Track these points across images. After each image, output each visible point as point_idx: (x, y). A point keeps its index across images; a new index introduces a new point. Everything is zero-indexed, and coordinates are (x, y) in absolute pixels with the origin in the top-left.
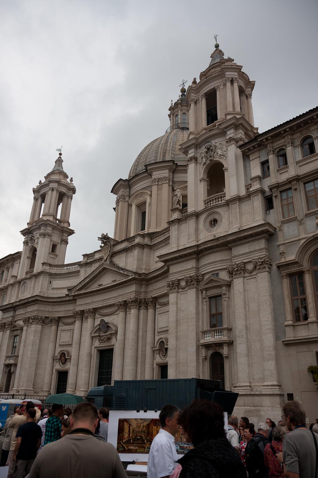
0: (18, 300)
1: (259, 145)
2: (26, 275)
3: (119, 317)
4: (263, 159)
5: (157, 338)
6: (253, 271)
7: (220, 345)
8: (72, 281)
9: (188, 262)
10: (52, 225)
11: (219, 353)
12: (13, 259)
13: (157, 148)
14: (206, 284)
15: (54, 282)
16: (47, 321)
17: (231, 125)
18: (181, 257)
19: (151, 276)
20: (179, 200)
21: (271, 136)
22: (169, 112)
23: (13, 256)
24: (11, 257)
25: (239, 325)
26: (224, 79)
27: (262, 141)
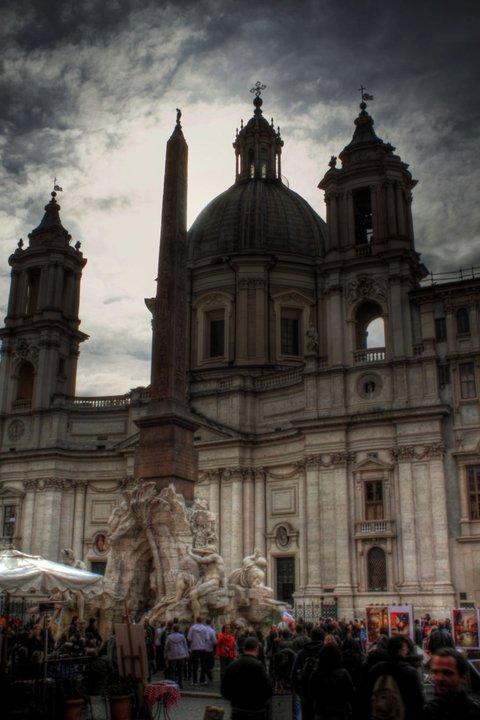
0: (8, 449)
3: (208, 490)
4: (439, 315)
5: (271, 523)
6: (424, 456)
7: (383, 539)
8: (106, 425)
9: (335, 434)
11: (381, 549)
14: (363, 465)
16: (68, 485)
17: (397, 257)
18: (325, 426)
19: (263, 438)
22: (234, 139)
25: (406, 517)
26: (383, 177)
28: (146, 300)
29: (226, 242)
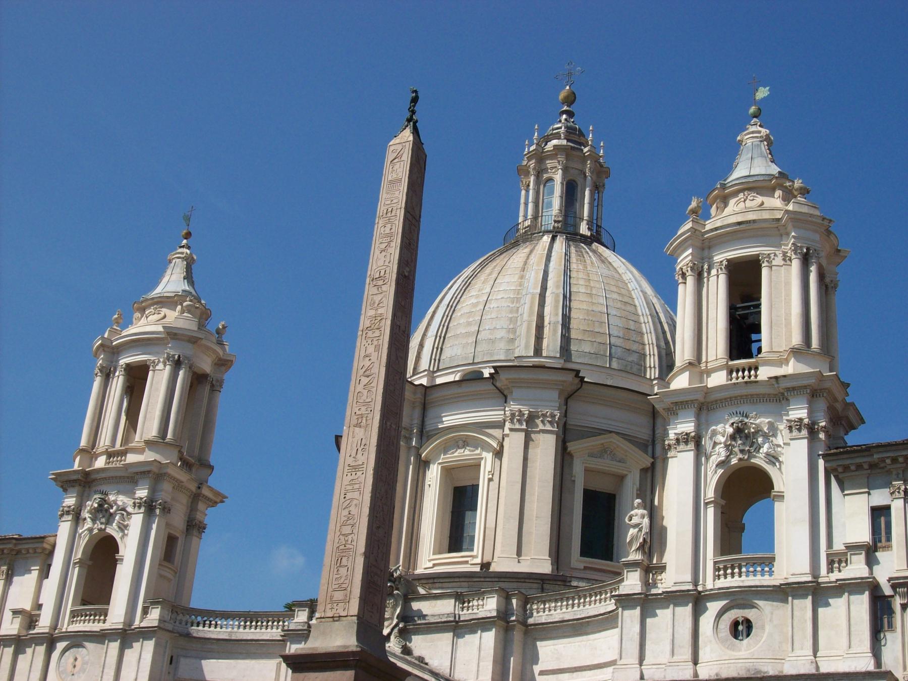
1: (872, 466)
2: (74, 617)
10: (174, 479)
12: (14, 553)
15: (183, 661)
17: (805, 387)
20: (644, 538)
23: (15, 545)
24: (10, 546)
27: (883, 460)
29: (492, 341)
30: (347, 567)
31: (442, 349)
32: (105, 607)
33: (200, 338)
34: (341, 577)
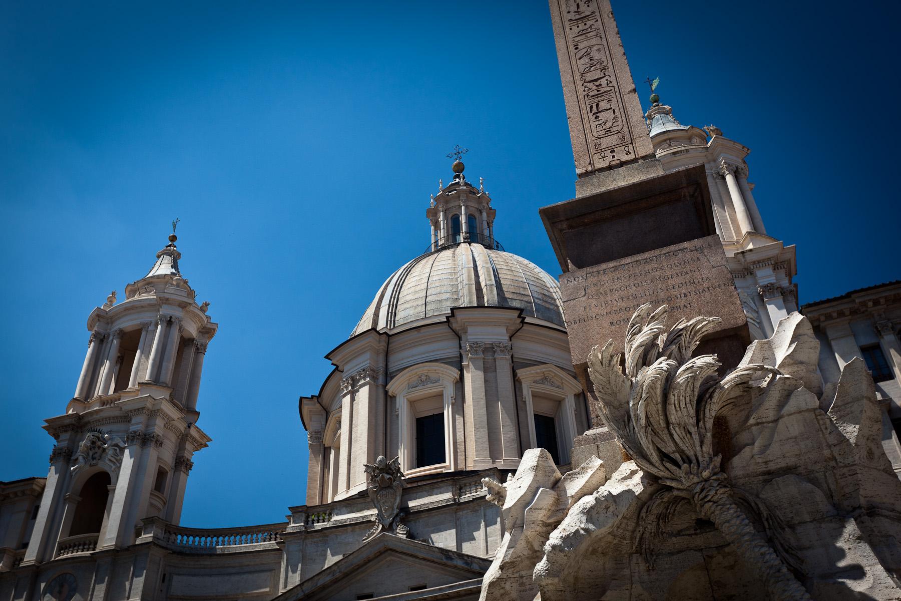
1: (854, 312)
13: (451, 274)
17: (770, 259)
21: (886, 297)
27: (864, 304)
28: (301, 398)
30: (611, 111)
31: (395, 314)
32: (96, 534)
33: (190, 304)
34: (605, 123)
